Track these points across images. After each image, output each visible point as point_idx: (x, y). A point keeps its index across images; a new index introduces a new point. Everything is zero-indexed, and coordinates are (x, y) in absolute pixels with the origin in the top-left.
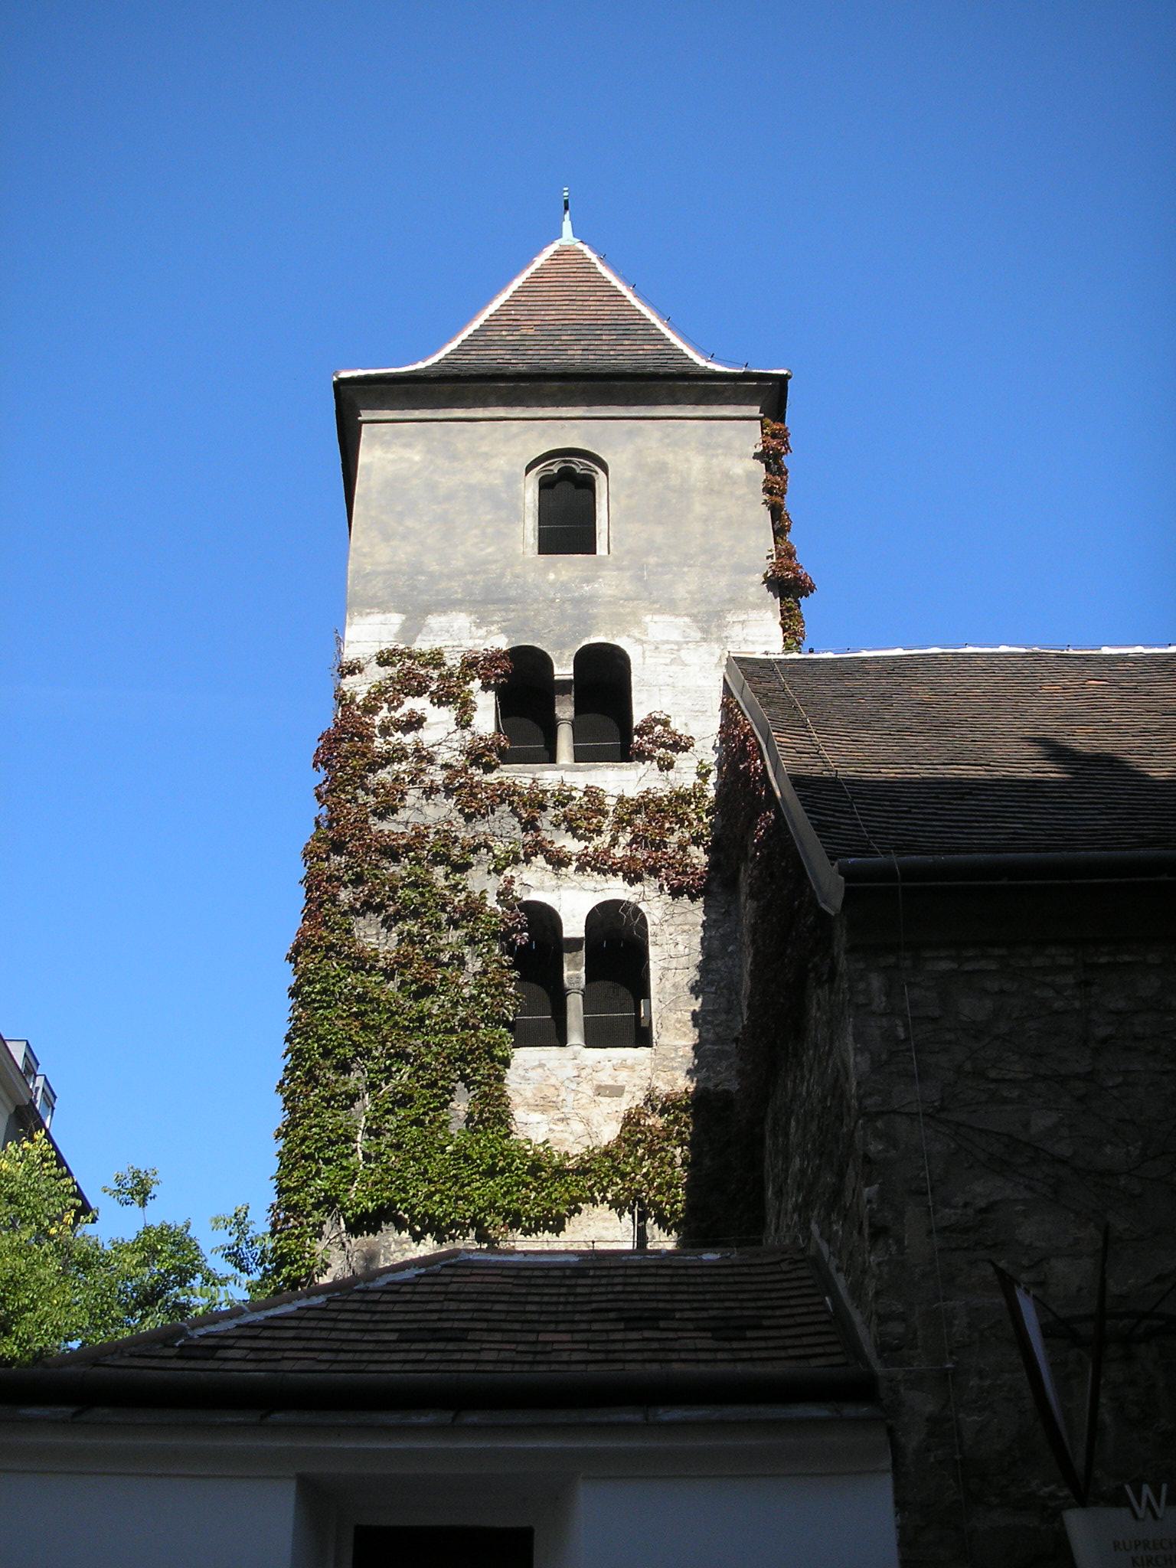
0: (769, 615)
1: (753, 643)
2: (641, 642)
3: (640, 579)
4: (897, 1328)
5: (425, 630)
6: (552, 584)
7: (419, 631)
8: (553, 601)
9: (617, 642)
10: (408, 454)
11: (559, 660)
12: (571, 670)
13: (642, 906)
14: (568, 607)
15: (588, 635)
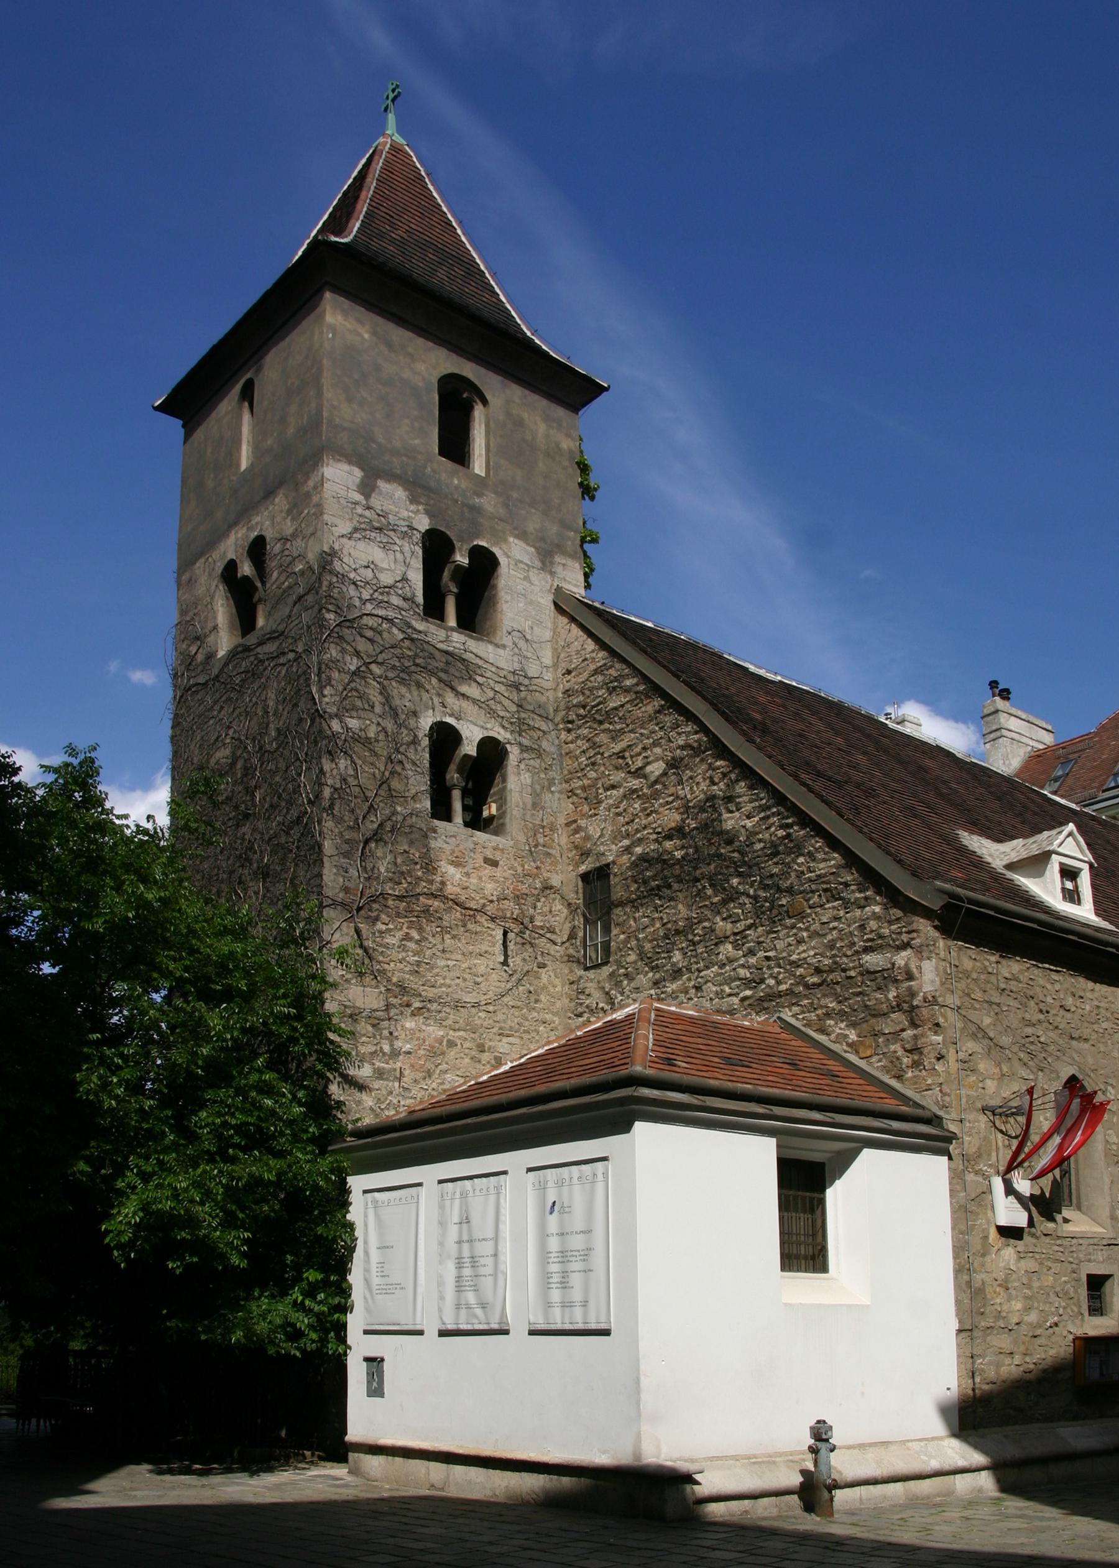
0: (577, 565)
1: (569, 583)
2: (508, 557)
3: (506, 506)
4: (947, 1098)
5: (377, 490)
6: (457, 488)
7: (373, 490)
8: (457, 501)
9: (495, 550)
10: (361, 330)
11: (460, 550)
12: (466, 561)
13: (508, 746)
14: (465, 509)
15: (477, 537)
